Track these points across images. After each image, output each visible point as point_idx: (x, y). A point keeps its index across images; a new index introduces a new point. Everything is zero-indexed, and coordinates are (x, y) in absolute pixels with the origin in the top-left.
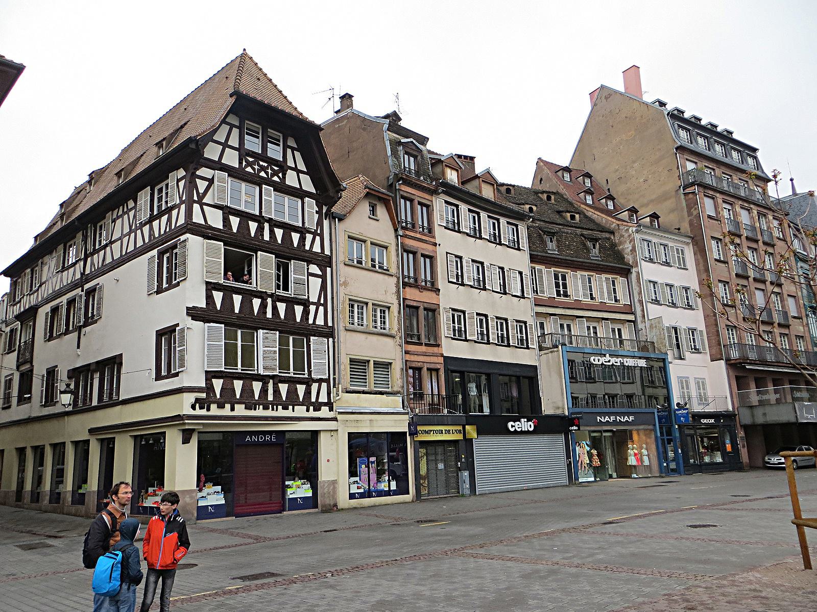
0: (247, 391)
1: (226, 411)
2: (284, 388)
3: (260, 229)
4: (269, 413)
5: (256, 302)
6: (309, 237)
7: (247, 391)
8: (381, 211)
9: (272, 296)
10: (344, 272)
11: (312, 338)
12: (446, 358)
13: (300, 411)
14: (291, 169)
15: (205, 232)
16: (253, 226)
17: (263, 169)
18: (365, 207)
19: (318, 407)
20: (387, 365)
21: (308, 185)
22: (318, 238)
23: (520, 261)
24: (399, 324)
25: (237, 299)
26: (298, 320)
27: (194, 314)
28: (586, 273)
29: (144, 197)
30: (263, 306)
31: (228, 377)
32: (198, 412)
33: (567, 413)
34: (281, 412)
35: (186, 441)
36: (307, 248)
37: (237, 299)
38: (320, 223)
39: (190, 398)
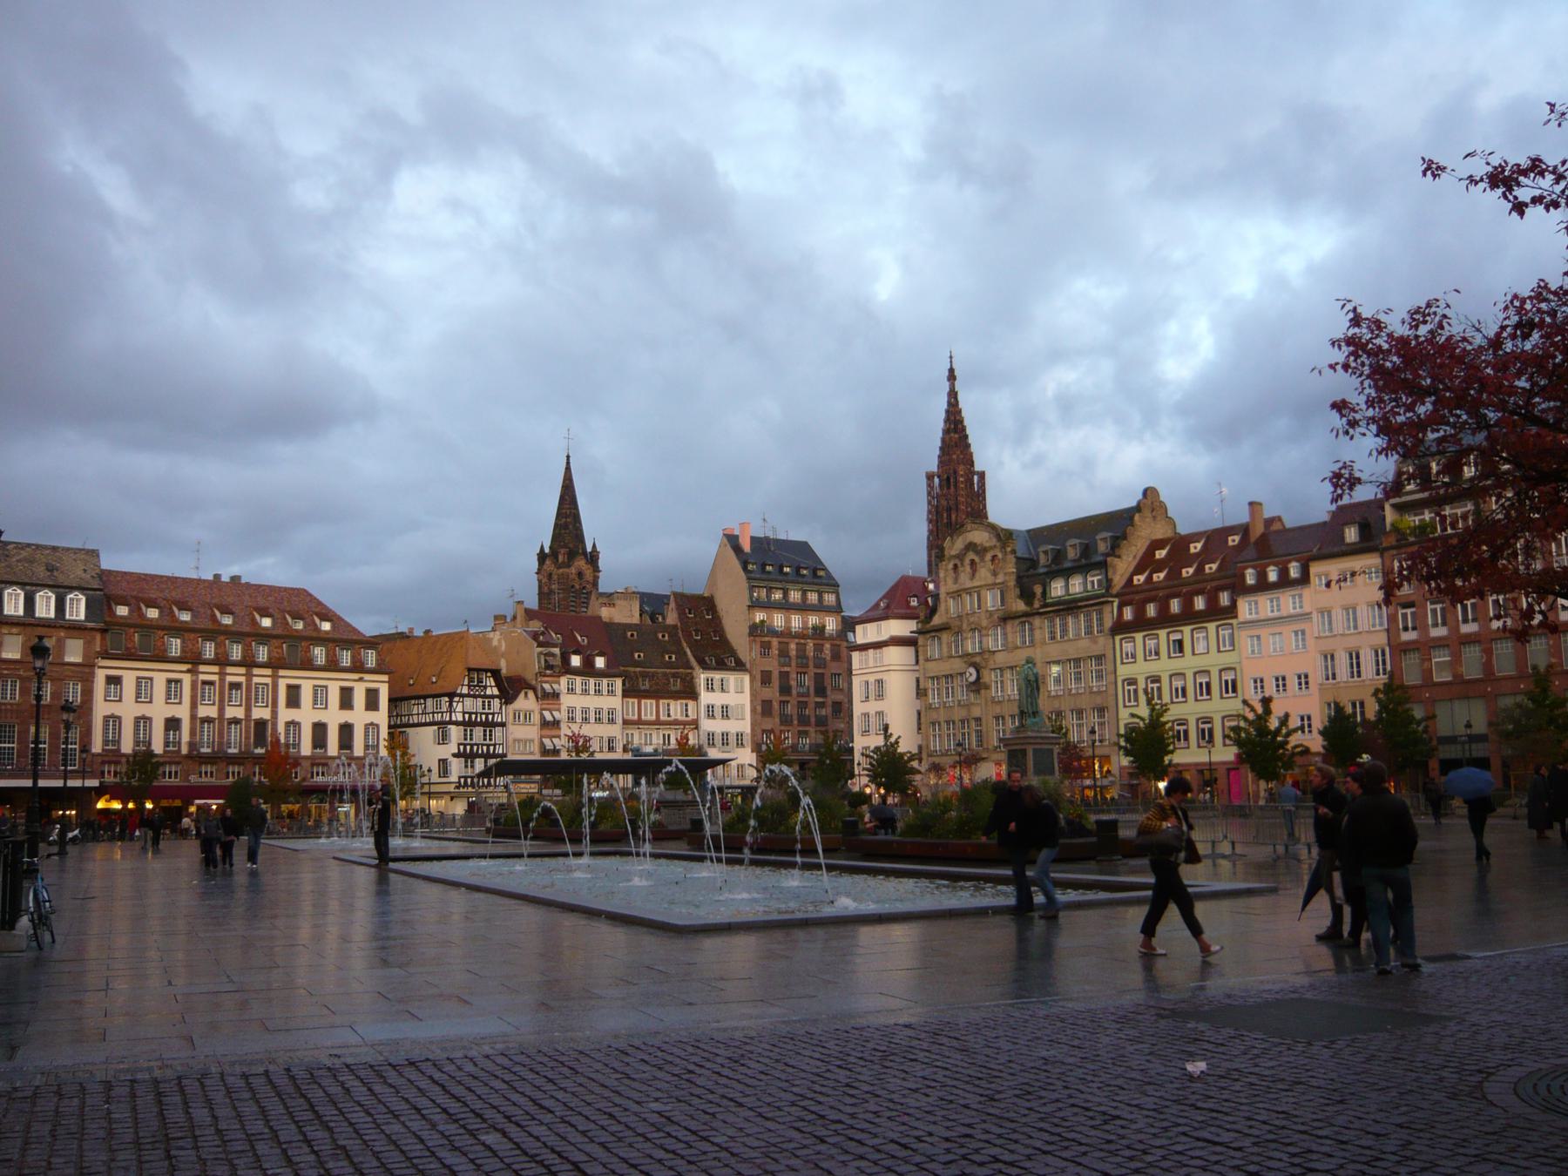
1: (465, 790)
3: (476, 718)
5: (475, 748)
8: (531, 694)
10: (510, 727)
15: (457, 723)
16: (474, 716)
21: (496, 692)
23: (615, 702)
25: (468, 747)
27: (454, 755)
28: (666, 701)
29: (429, 701)
31: (466, 778)
37: (468, 747)
38: (501, 708)
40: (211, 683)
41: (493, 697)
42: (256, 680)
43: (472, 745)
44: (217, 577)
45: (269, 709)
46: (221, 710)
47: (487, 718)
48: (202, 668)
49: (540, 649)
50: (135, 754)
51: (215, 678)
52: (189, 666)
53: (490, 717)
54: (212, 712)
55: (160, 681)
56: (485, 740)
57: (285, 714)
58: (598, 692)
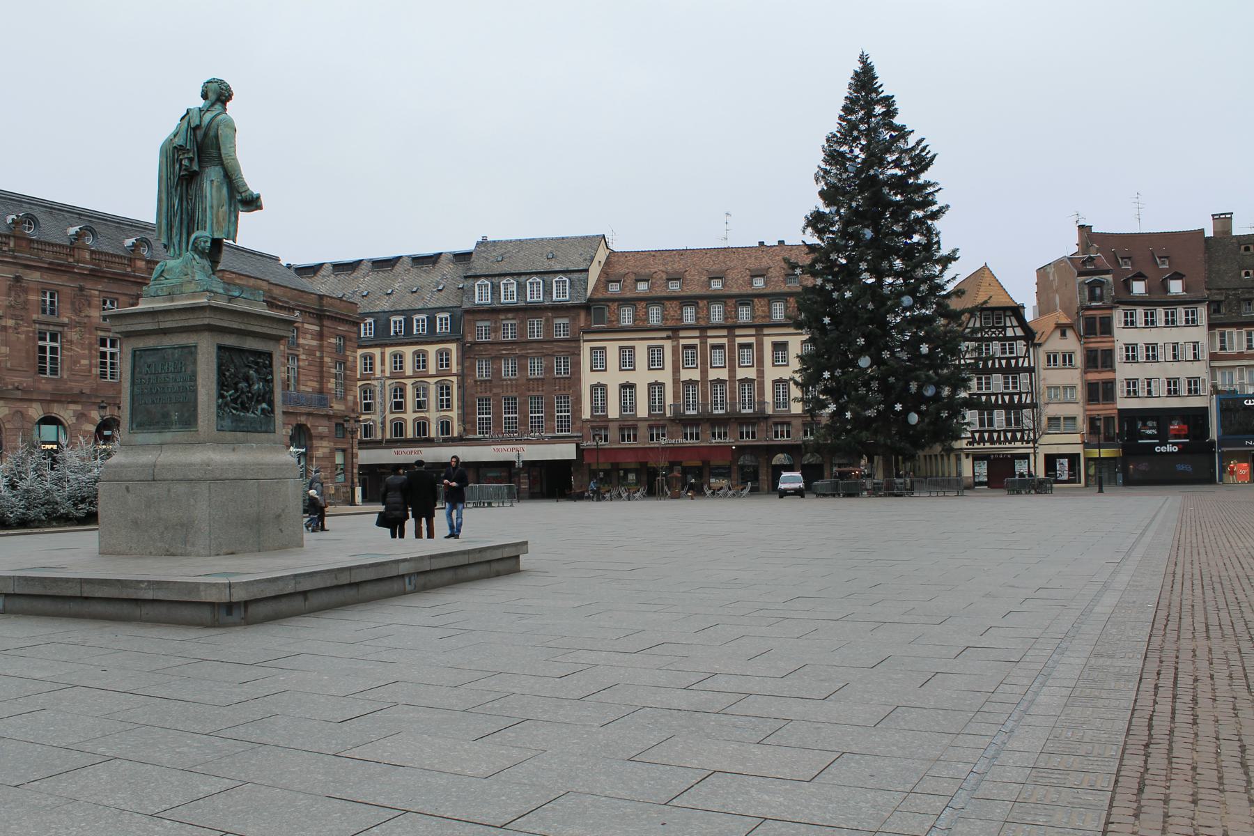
0: (991, 437)
1: (981, 446)
2: (1009, 435)
4: (1002, 446)
5: (993, 398)
6: (1021, 360)
7: (991, 437)
9: (1000, 393)
10: (1043, 373)
11: (1023, 410)
12: (1119, 410)
13: (1018, 444)
14: (1009, 327)
17: (994, 332)
18: (1058, 333)
19: (1028, 442)
20: (1074, 419)
21: (1019, 332)
22: (1027, 359)
23: (1200, 334)
24: (1082, 394)
26: (1016, 402)
30: (997, 400)
32: (969, 447)
33: (1216, 439)
34: (1008, 445)
35: (967, 457)
36: (1020, 365)
38: (1028, 350)
39: (965, 441)
40: (694, 347)
41: (1016, 338)
42: (739, 340)
43: (989, 395)
44: (761, 244)
45: (755, 368)
46: (704, 373)
47: (1008, 363)
48: (682, 334)
49: (1081, 279)
50: (622, 418)
51: (697, 341)
52: (670, 333)
53: (1013, 362)
54: (695, 375)
55: (641, 349)
56: (1006, 388)
57: (771, 374)
58: (1171, 323)
